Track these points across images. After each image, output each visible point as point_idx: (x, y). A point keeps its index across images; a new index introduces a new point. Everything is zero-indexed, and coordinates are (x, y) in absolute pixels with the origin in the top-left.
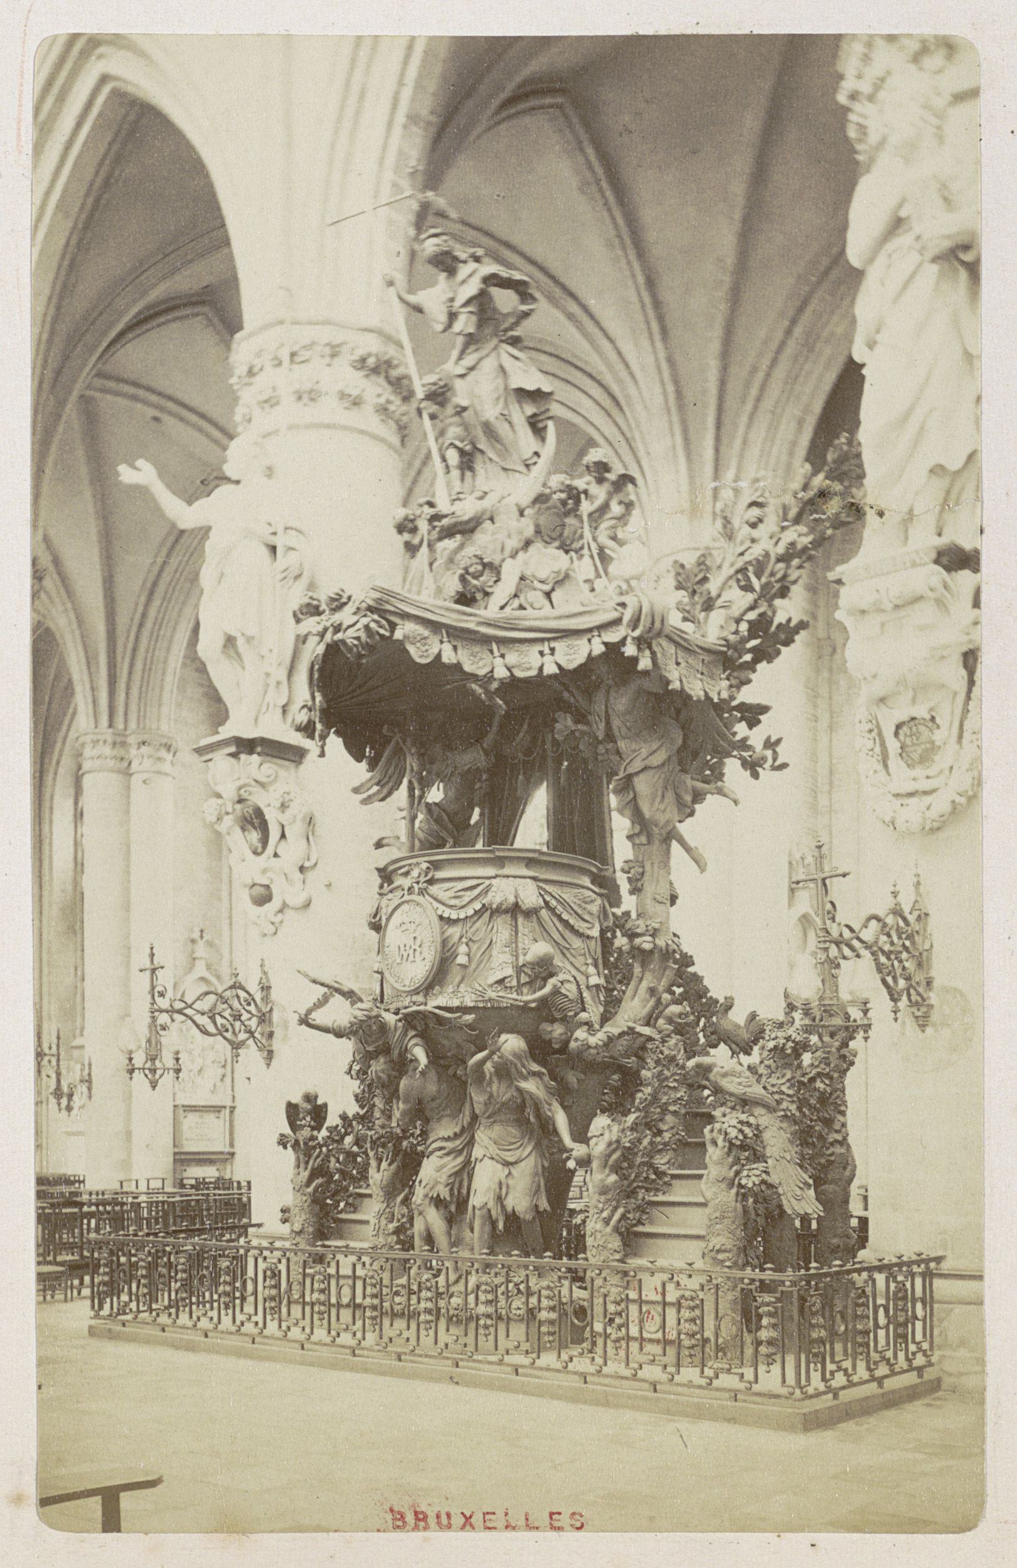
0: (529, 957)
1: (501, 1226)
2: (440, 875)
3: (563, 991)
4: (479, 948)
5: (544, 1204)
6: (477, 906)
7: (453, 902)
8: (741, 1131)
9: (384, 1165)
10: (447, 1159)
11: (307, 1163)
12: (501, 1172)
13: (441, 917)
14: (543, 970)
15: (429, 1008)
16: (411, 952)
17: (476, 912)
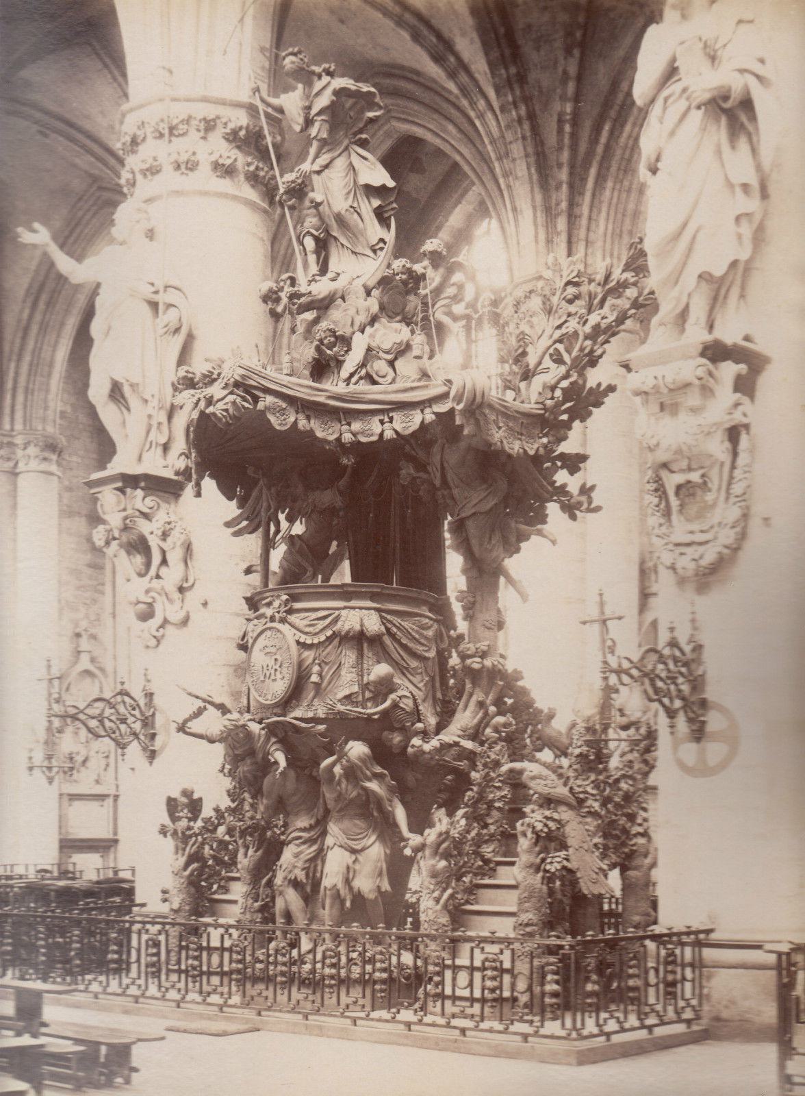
0: (372, 677)
1: (348, 904)
2: (297, 605)
3: (402, 705)
4: (330, 669)
5: (386, 886)
6: (329, 633)
7: (307, 630)
8: (546, 825)
9: (251, 852)
10: (303, 847)
11: (184, 849)
12: (348, 858)
13: (298, 642)
14: (384, 688)
15: (288, 719)
16: (273, 671)
17: (328, 638)
